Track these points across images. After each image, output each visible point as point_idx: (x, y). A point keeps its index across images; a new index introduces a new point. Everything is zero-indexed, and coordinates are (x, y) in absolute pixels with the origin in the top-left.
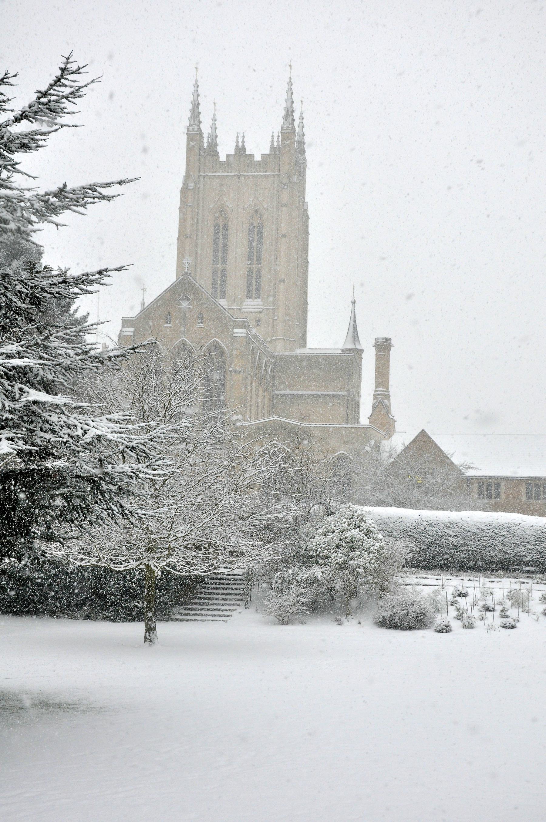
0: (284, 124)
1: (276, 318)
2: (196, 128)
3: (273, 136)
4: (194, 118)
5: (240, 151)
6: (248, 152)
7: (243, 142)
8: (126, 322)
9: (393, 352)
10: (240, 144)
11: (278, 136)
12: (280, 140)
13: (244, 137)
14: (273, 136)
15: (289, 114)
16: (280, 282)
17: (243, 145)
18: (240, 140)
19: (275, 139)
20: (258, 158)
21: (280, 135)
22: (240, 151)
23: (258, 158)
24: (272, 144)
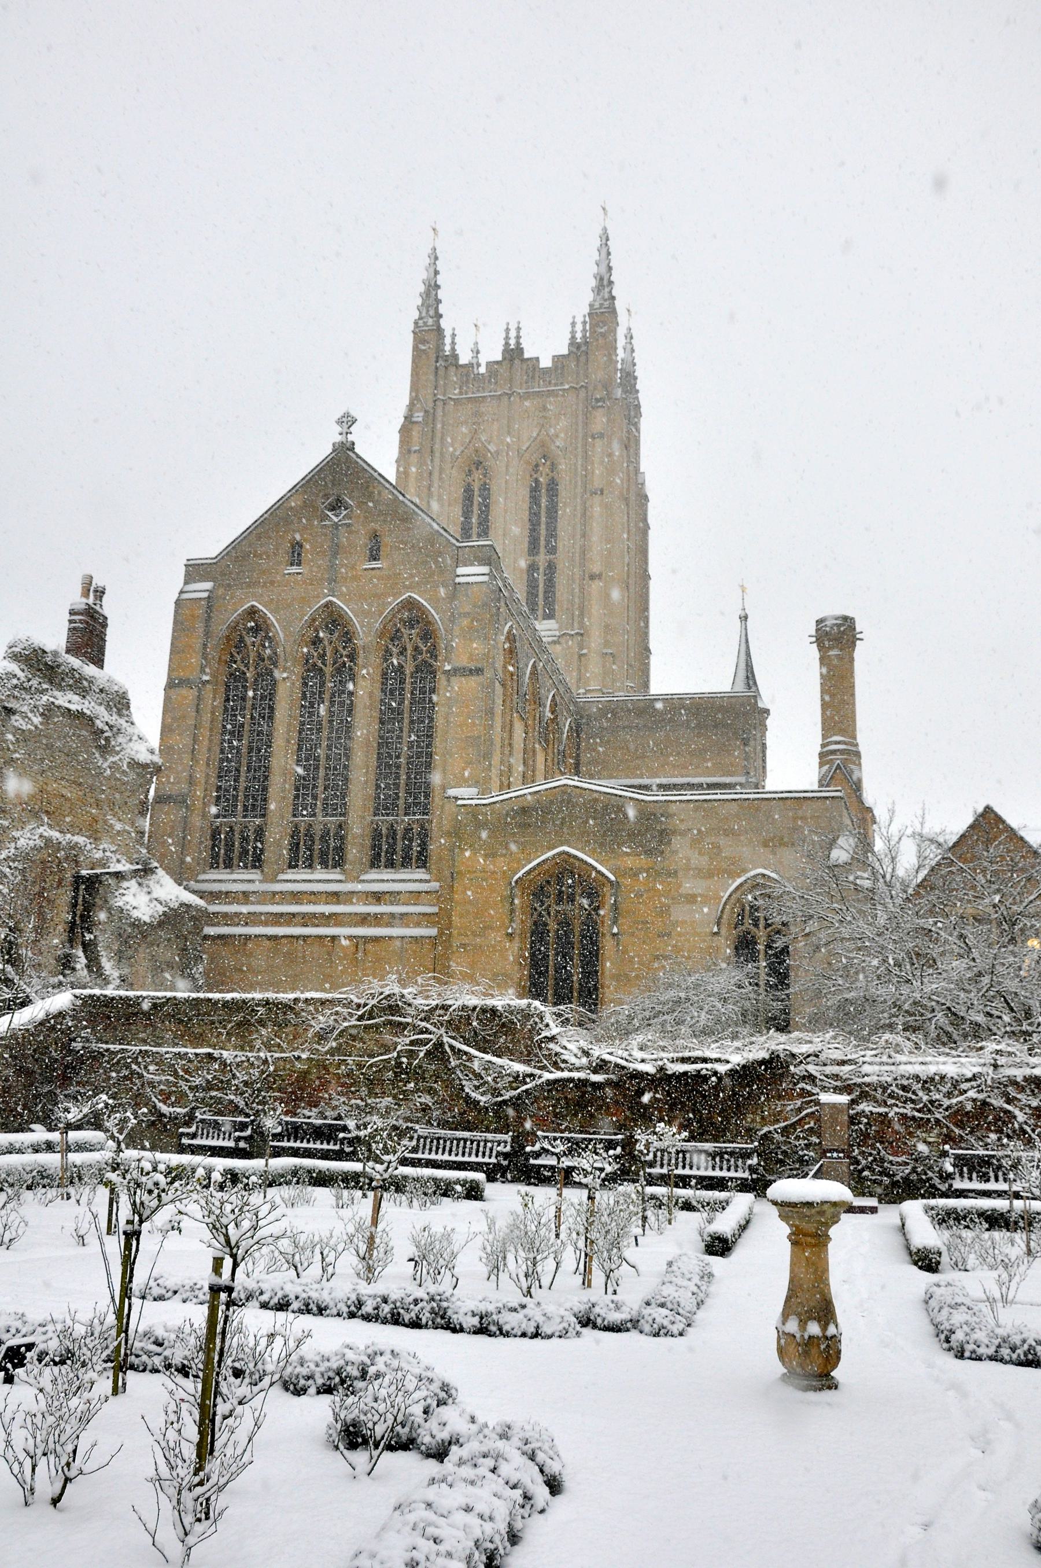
0: (594, 301)
1: (585, 651)
2: (430, 321)
3: (573, 324)
4: (428, 306)
5: (513, 354)
6: (526, 355)
7: (518, 337)
8: (195, 571)
9: (861, 652)
10: (512, 342)
11: (584, 323)
12: (588, 328)
13: (519, 329)
14: (573, 324)
15: (604, 283)
16: (592, 577)
17: (518, 343)
18: (513, 334)
19: (579, 327)
20: (546, 363)
21: (587, 319)
22: (513, 354)
23: (546, 363)
24: (573, 337)
